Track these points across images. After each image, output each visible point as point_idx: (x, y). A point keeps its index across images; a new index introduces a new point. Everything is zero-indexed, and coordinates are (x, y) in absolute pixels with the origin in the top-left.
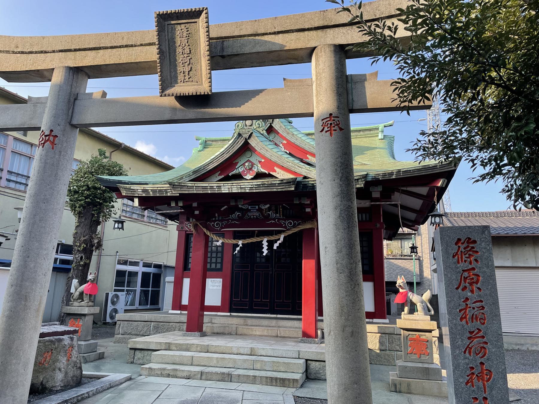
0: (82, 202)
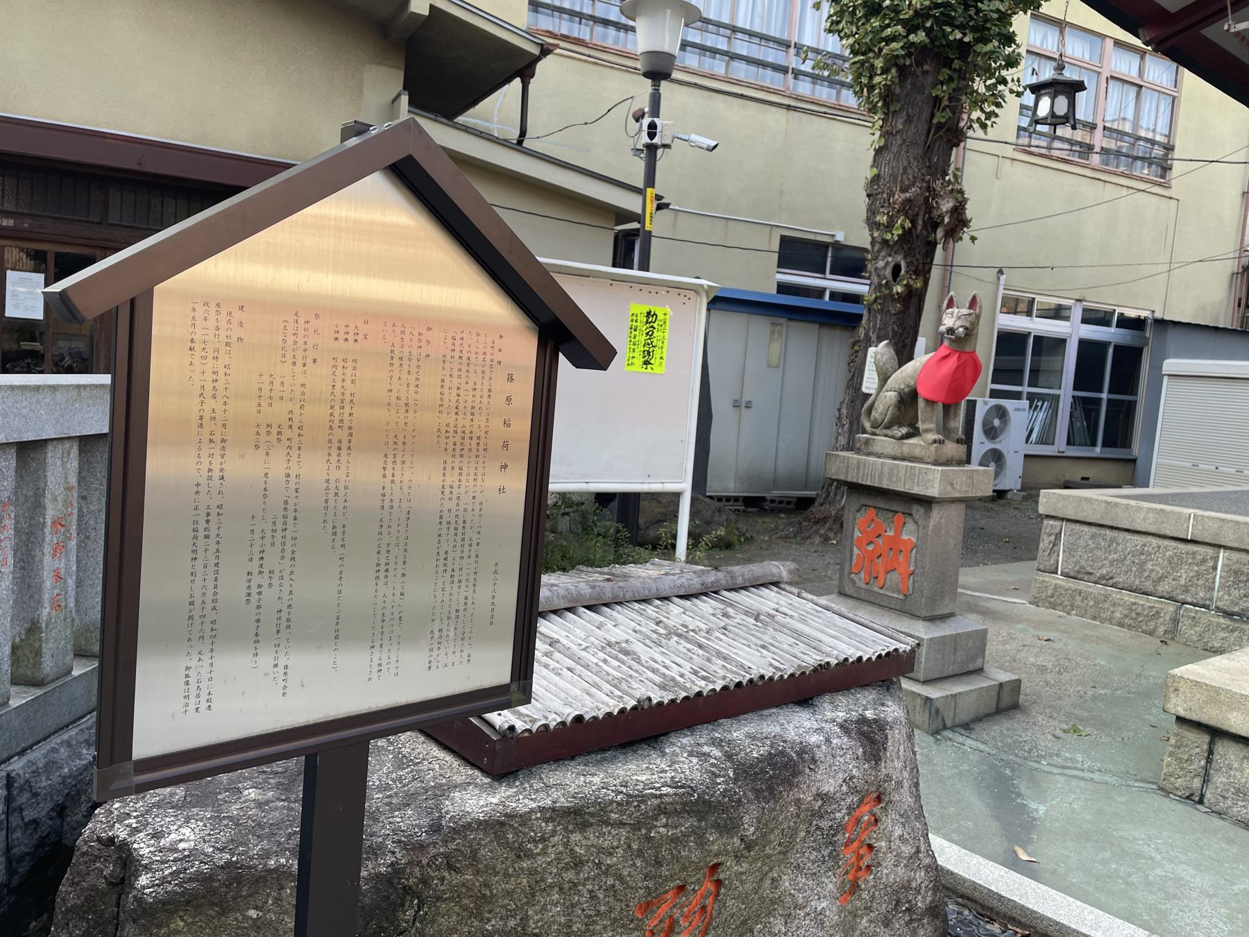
0: (894, 45)
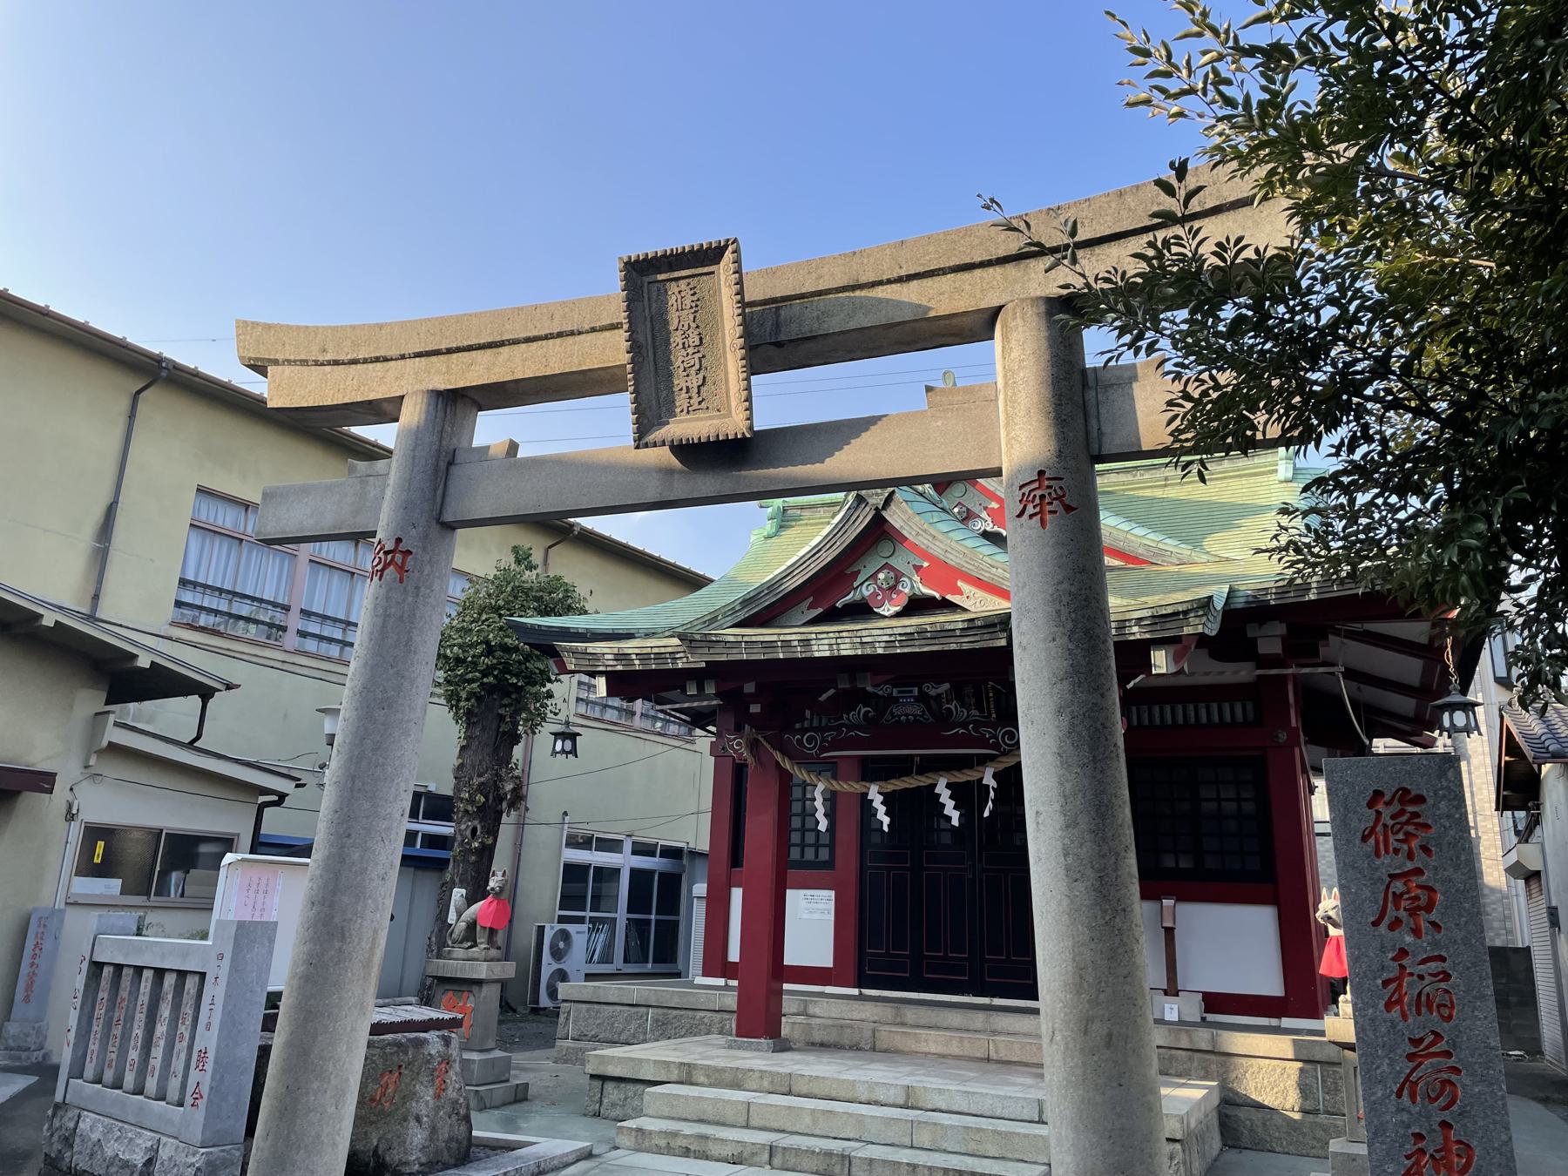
0: (475, 685)
